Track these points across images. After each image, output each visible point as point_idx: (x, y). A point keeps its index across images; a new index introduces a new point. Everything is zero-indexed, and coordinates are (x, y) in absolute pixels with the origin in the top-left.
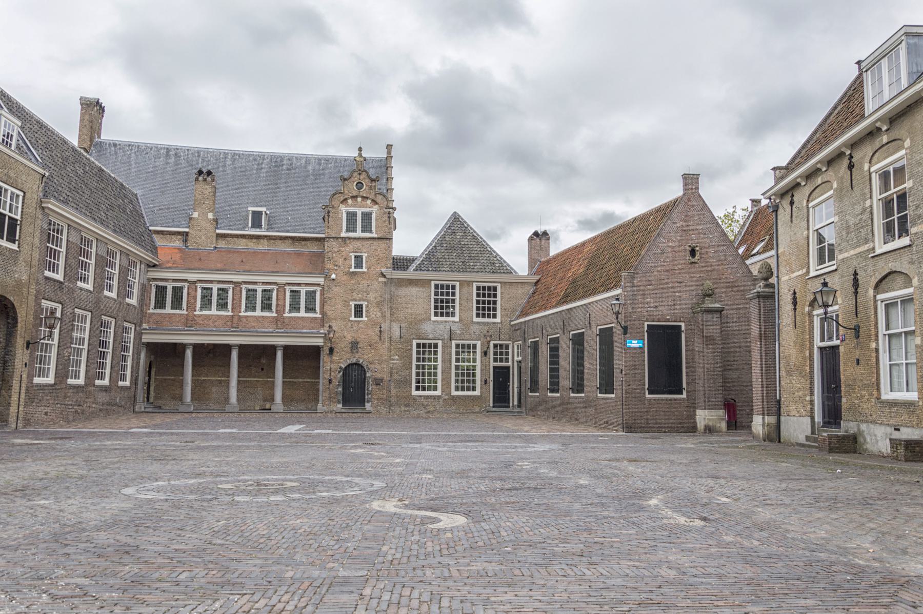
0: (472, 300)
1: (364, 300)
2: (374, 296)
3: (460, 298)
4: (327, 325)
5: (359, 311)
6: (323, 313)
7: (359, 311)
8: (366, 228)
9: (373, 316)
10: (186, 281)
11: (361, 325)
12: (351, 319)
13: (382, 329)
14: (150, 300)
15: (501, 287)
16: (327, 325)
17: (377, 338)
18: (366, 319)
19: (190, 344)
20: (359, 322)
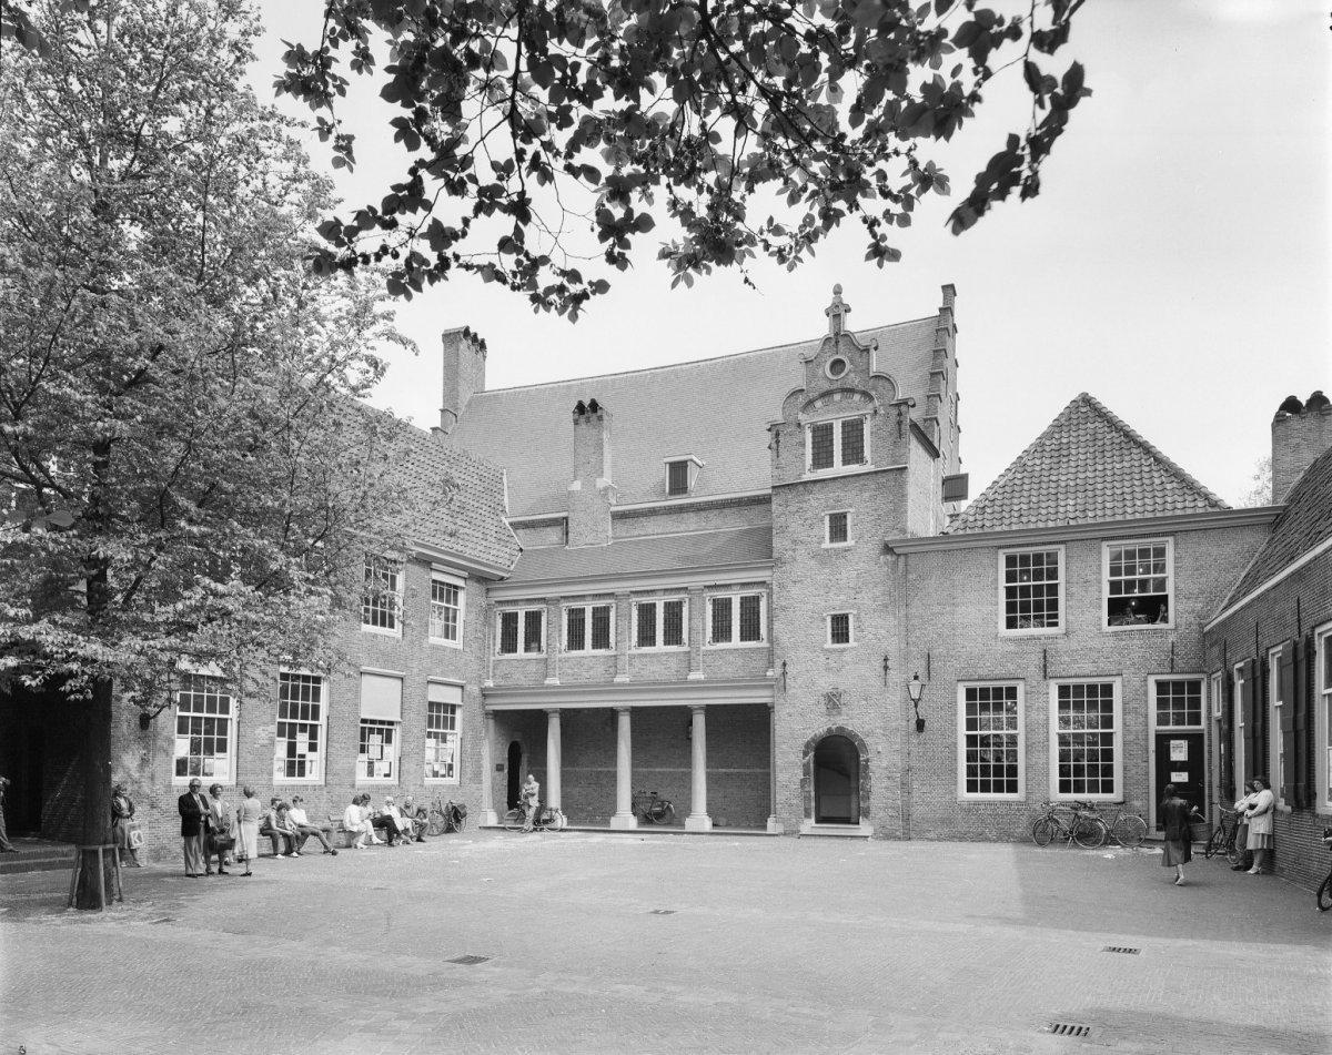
0: (1100, 582)
1: (852, 607)
2: (870, 595)
3: (1067, 582)
4: (778, 663)
5: (840, 628)
6: (771, 640)
7: (840, 628)
8: (853, 453)
9: (871, 636)
10: (543, 600)
11: (847, 657)
12: (826, 646)
13: (889, 663)
14: (494, 639)
15: (1176, 544)
16: (778, 663)
17: (879, 683)
18: (855, 644)
19: (555, 711)
20: (843, 650)
